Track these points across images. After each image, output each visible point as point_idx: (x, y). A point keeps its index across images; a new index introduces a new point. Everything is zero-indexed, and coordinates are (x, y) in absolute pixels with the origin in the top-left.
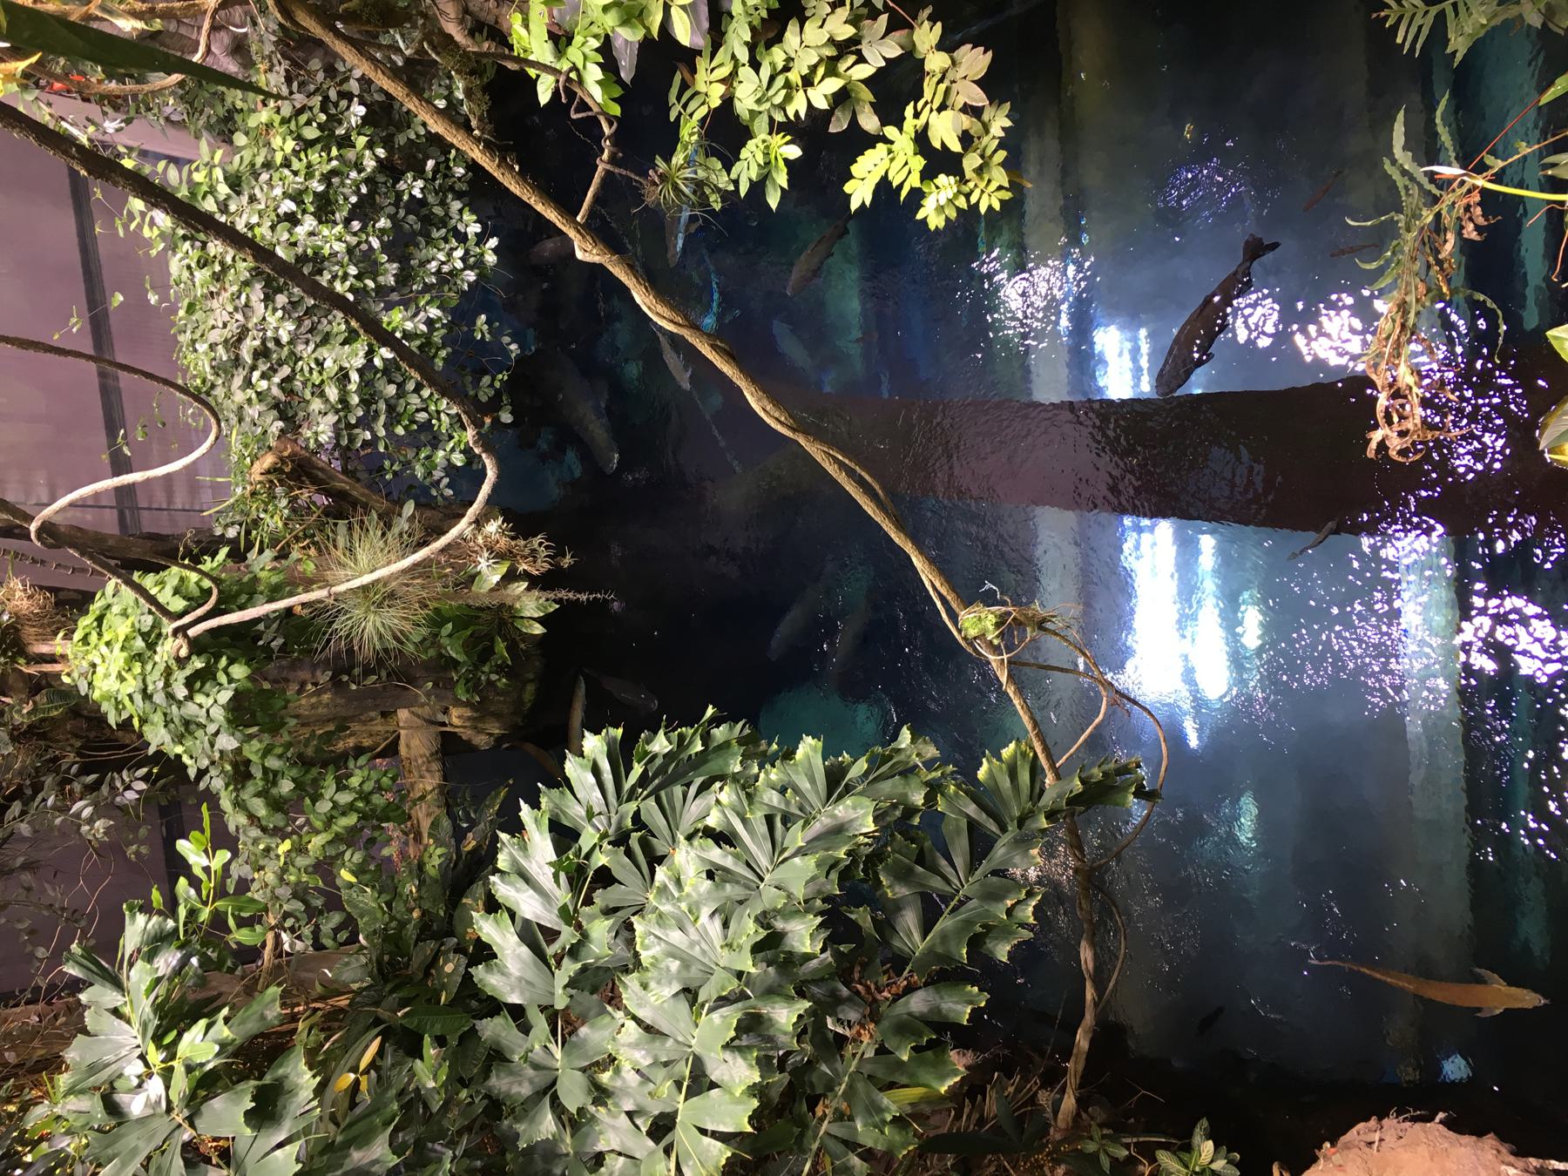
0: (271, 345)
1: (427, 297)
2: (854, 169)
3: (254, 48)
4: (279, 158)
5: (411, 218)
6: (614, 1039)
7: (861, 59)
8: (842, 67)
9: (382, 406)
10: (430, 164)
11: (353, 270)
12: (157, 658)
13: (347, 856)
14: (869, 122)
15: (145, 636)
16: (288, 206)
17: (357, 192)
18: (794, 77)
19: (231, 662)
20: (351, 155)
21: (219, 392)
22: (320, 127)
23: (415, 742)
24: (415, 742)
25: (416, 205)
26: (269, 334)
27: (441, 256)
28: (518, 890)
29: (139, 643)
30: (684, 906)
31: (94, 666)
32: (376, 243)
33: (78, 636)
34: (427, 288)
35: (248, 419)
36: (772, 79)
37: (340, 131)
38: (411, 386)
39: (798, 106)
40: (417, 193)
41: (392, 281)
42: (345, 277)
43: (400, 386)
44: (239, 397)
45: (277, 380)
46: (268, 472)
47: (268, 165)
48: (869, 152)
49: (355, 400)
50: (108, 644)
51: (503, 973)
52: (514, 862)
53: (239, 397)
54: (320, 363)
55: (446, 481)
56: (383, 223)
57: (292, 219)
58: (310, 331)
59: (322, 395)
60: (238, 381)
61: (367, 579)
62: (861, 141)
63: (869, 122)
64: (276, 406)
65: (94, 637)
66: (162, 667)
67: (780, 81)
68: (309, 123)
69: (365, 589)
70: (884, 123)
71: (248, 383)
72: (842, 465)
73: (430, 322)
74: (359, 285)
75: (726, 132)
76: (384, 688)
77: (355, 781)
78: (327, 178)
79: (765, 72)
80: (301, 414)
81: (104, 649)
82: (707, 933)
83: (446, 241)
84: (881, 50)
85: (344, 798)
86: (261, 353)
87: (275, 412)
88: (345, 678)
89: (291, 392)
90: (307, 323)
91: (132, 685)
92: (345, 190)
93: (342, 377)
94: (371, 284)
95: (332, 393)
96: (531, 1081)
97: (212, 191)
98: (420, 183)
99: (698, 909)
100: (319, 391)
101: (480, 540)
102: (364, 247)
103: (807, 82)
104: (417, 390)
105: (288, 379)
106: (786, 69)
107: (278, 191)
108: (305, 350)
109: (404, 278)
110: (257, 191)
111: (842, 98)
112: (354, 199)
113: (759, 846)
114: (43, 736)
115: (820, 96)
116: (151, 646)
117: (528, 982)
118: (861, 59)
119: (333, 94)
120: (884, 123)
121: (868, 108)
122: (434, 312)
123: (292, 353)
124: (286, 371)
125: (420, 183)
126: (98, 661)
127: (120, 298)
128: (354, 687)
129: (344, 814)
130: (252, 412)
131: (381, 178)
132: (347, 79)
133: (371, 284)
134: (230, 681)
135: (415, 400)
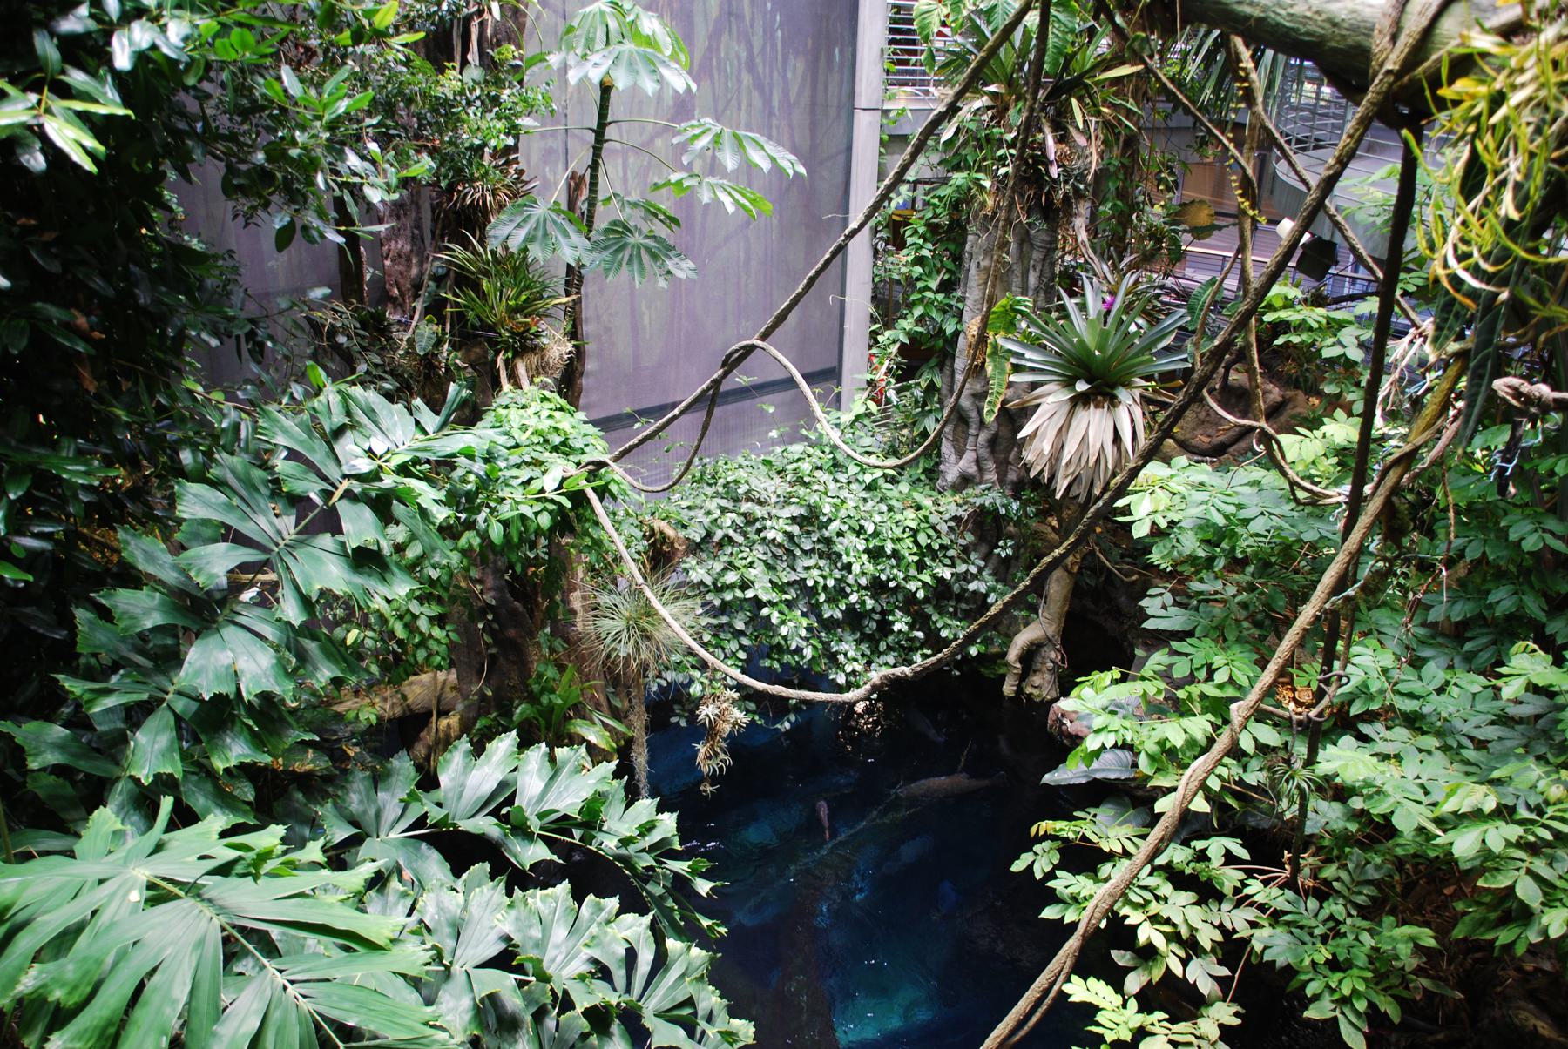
0: (758, 525)
2: (1092, 980)
3: (970, 491)
4: (899, 517)
5: (874, 625)
7: (1185, 963)
8: (1174, 947)
9: (724, 620)
10: (920, 635)
11: (830, 583)
13: (370, 633)
14: (1133, 983)
15: (564, 444)
17: (889, 580)
18: (1154, 908)
19: (551, 512)
20: (913, 572)
21: (709, 491)
22: (929, 546)
23: (417, 689)
24: (417, 689)
25: (885, 627)
26: (768, 524)
28: (539, 770)
29: (557, 440)
30: (594, 929)
31: (524, 407)
32: (854, 598)
33: (547, 393)
34: (826, 645)
35: (692, 513)
36: (1145, 888)
37: (928, 561)
38: (745, 641)
39: (1134, 917)
40: (896, 627)
42: (825, 578)
44: (712, 505)
45: (731, 532)
46: (662, 533)
47: (890, 509)
48: (1110, 990)
49: (728, 596)
50: (550, 416)
51: (467, 770)
52: (565, 763)
53: (712, 505)
54: (751, 565)
55: (664, 684)
56: (870, 603)
57: (860, 531)
58: (774, 555)
59: (726, 569)
60: (724, 503)
61: (664, 612)
62: (1115, 978)
63: (1133, 983)
64: (709, 535)
65: (547, 405)
66: (542, 458)
67: (1148, 896)
68: (929, 537)
69: (649, 612)
70: (1137, 996)
71: (724, 510)
73: (799, 651)
75: (1083, 858)
76: (480, 653)
77: (437, 632)
78: (895, 554)
79: (1152, 881)
80: (704, 556)
81: (545, 413)
82: (572, 959)
83: (863, 655)
84: (1202, 974)
85: (423, 624)
86: (750, 520)
87: (704, 533)
88: (490, 617)
89: (720, 545)
90: (780, 552)
93: (745, 585)
94: (822, 598)
95: (731, 577)
96: (365, 812)
97: (864, 471)
98: (905, 628)
99: (598, 945)
100: (730, 566)
101: (725, 705)
102: (848, 590)
103: (1155, 919)
104: (742, 647)
105: (731, 540)
106: (1157, 898)
107: (878, 518)
108: (759, 552)
109: (830, 625)
110: (870, 504)
111: (1148, 954)
112: (883, 577)
113: (665, 996)
114: (427, 377)
115: (1147, 933)
116: (555, 449)
117: (461, 793)
118: (1185, 963)
119: (951, 553)
120: (1137, 996)
121: (1144, 980)
122: (808, 652)
123: (754, 542)
124: (739, 539)
125: (905, 628)
126: (530, 411)
127: (771, 410)
128: (481, 626)
129: (406, 626)
130: (700, 514)
131: (900, 597)
132: (964, 562)
133: (822, 598)
134: (536, 514)
135: (734, 646)
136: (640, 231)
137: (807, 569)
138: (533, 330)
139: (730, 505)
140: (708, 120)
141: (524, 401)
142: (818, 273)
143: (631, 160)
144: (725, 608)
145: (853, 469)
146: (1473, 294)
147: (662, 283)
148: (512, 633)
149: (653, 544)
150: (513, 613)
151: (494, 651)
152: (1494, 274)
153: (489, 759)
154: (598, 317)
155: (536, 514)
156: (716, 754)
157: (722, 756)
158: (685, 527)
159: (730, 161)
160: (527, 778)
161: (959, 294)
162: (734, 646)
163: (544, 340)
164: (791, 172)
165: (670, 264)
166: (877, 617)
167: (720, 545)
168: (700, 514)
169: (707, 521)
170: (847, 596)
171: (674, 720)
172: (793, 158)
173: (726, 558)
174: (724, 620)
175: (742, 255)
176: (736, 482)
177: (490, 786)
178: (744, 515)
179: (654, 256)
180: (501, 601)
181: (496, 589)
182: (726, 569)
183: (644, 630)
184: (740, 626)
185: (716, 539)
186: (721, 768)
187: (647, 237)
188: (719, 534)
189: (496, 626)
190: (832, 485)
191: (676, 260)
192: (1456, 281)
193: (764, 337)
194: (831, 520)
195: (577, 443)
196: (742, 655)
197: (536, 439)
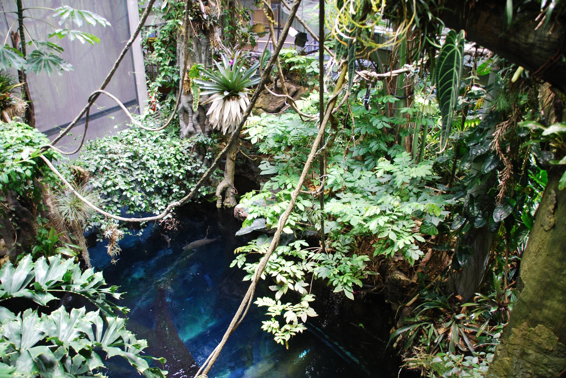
0: (116, 162)
1: (147, 202)
2: (264, 298)
3: (193, 137)
4: (168, 150)
5: (166, 191)
6: (10, 320)
7: (294, 284)
8: (289, 280)
9: (109, 199)
10: (184, 192)
11: (147, 179)
12: (24, 147)
14: (278, 296)
15: (31, 142)
16: (158, 156)
17: (169, 174)
18: (281, 269)
19: (30, 169)
20: (177, 169)
21: (95, 152)
22: (181, 159)
25: (170, 191)
26: (120, 161)
27: (159, 203)
28: (43, 267)
29: (27, 141)
30: (77, 321)
31: (10, 130)
32: (157, 183)
33: (19, 123)
34: (150, 201)
35: (89, 162)
36: (276, 263)
37: (182, 165)
38: (119, 206)
39: (274, 273)
40: (174, 191)
41: (148, 191)
42: (144, 177)
43: (117, 203)
44: (97, 157)
45: (106, 166)
46: (79, 171)
48: (271, 299)
49: (109, 190)
51: (12, 274)
52: (53, 262)
53: (97, 157)
54: (116, 177)
55: (91, 227)
56: (163, 183)
57: (155, 158)
58: (124, 172)
59: (106, 180)
60: (101, 156)
61: (84, 199)
62: (272, 295)
63: (278, 296)
64: (97, 169)
65: (20, 127)
67: (278, 265)
68: (180, 156)
69: (78, 201)
70: (280, 300)
71: (102, 158)
72: (247, 303)
74: (144, 182)
75: (254, 257)
76: (12, 230)
78: (169, 164)
79: (278, 260)
80: (97, 177)
81: (20, 131)
82: (71, 334)
83: (164, 203)
84: (300, 287)
86: (112, 160)
87: (95, 168)
88: (14, 215)
89: (103, 172)
90: (126, 171)
91: (12, 142)
92: (168, 171)
93: (115, 185)
94: (145, 184)
95: (109, 183)
97: (152, 136)
98: (178, 190)
99: (80, 326)
100: (108, 179)
101: (114, 229)
102: (154, 180)
103: (281, 273)
104: (118, 208)
105: (107, 170)
106: (281, 265)
107: (160, 152)
108: (118, 172)
109: (150, 194)
110: (157, 147)
111: (282, 284)
112: (166, 173)
113: (110, 338)
115: (280, 278)
116: (27, 144)
118: (294, 284)
119: (189, 160)
120: (280, 300)
121: (282, 294)
122: (144, 206)
123: (115, 169)
125: (178, 190)
127: (113, 118)
128: (10, 219)
130: (93, 162)
131: (174, 179)
132: (195, 163)
133: (145, 184)
134: (24, 171)
135: (115, 208)
136: (47, 54)
137: (137, 175)
138: (8, 98)
139: (104, 156)
140: (67, 6)
141: (10, 127)
142: (120, 61)
143: (38, 26)
144: (109, 195)
145: (148, 136)
146: (346, 41)
147: (60, 74)
148: (25, 220)
149: (76, 176)
150: (24, 212)
151: (18, 228)
152: (351, 33)
153: (21, 267)
154: (37, 91)
155: (24, 171)
156: (115, 248)
157: (117, 248)
158: (87, 167)
159: (79, 23)
160: (39, 271)
161: (177, 66)
162: (115, 208)
163: (14, 102)
164: (105, 25)
165: (62, 66)
166: (167, 188)
167: (103, 172)
168: (93, 162)
169: (96, 163)
170: (154, 182)
171: (98, 240)
172: (104, 19)
173: (106, 176)
174: (109, 199)
175: (92, 60)
176: (104, 147)
177: (24, 277)
178: (110, 159)
179: (55, 63)
180: (17, 208)
181: (15, 204)
182: (106, 180)
183: (78, 208)
184: (116, 200)
185: (101, 169)
186: (117, 253)
187: (50, 56)
188: (101, 168)
189: (17, 218)
190: (141, 143)
191: (64, 64)
192: (341, 37)
193: (103, 88)
194: (143, 156)
195: (36, 141)
196: (119, 211)
197: (18, 142)
